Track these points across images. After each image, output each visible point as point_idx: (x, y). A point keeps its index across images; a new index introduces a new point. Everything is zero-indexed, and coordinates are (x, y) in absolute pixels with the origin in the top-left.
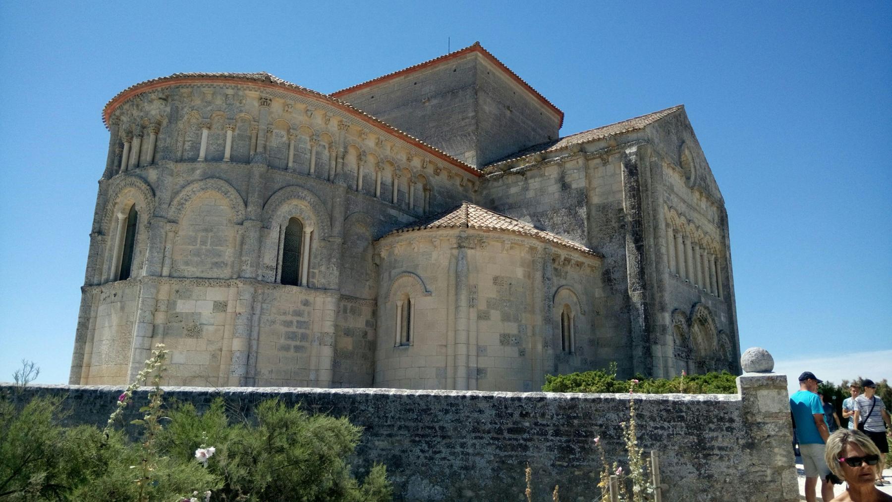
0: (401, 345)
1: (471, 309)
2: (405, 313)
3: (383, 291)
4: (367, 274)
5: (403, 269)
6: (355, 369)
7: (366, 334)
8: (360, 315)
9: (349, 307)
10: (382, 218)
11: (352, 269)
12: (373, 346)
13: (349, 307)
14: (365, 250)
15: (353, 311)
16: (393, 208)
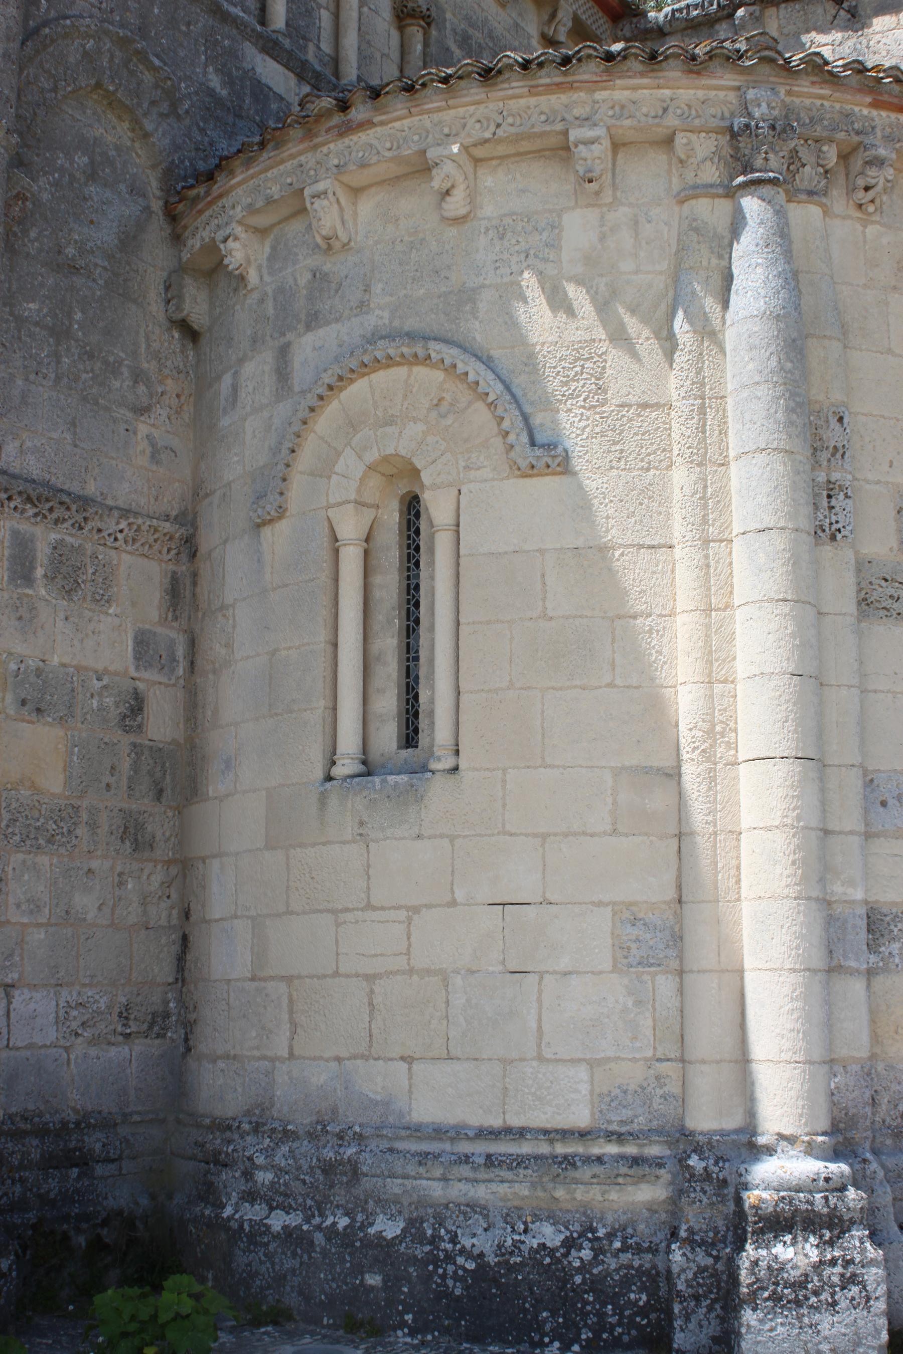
0: (368, 768)
1: (828, 550)
2: (389, 584)
3: (244, 454)
4: (138, 376)
5: (378, 317)
6: (86, 903)
7: (136, 706)
8: (103, 600)
9: (42, 552)
10: (215, 81)
11: (60, 333)
12: (176, 776)
13: (42, 552)
14: (129, 241)
15: (68, 575)
16: (270, 47)
